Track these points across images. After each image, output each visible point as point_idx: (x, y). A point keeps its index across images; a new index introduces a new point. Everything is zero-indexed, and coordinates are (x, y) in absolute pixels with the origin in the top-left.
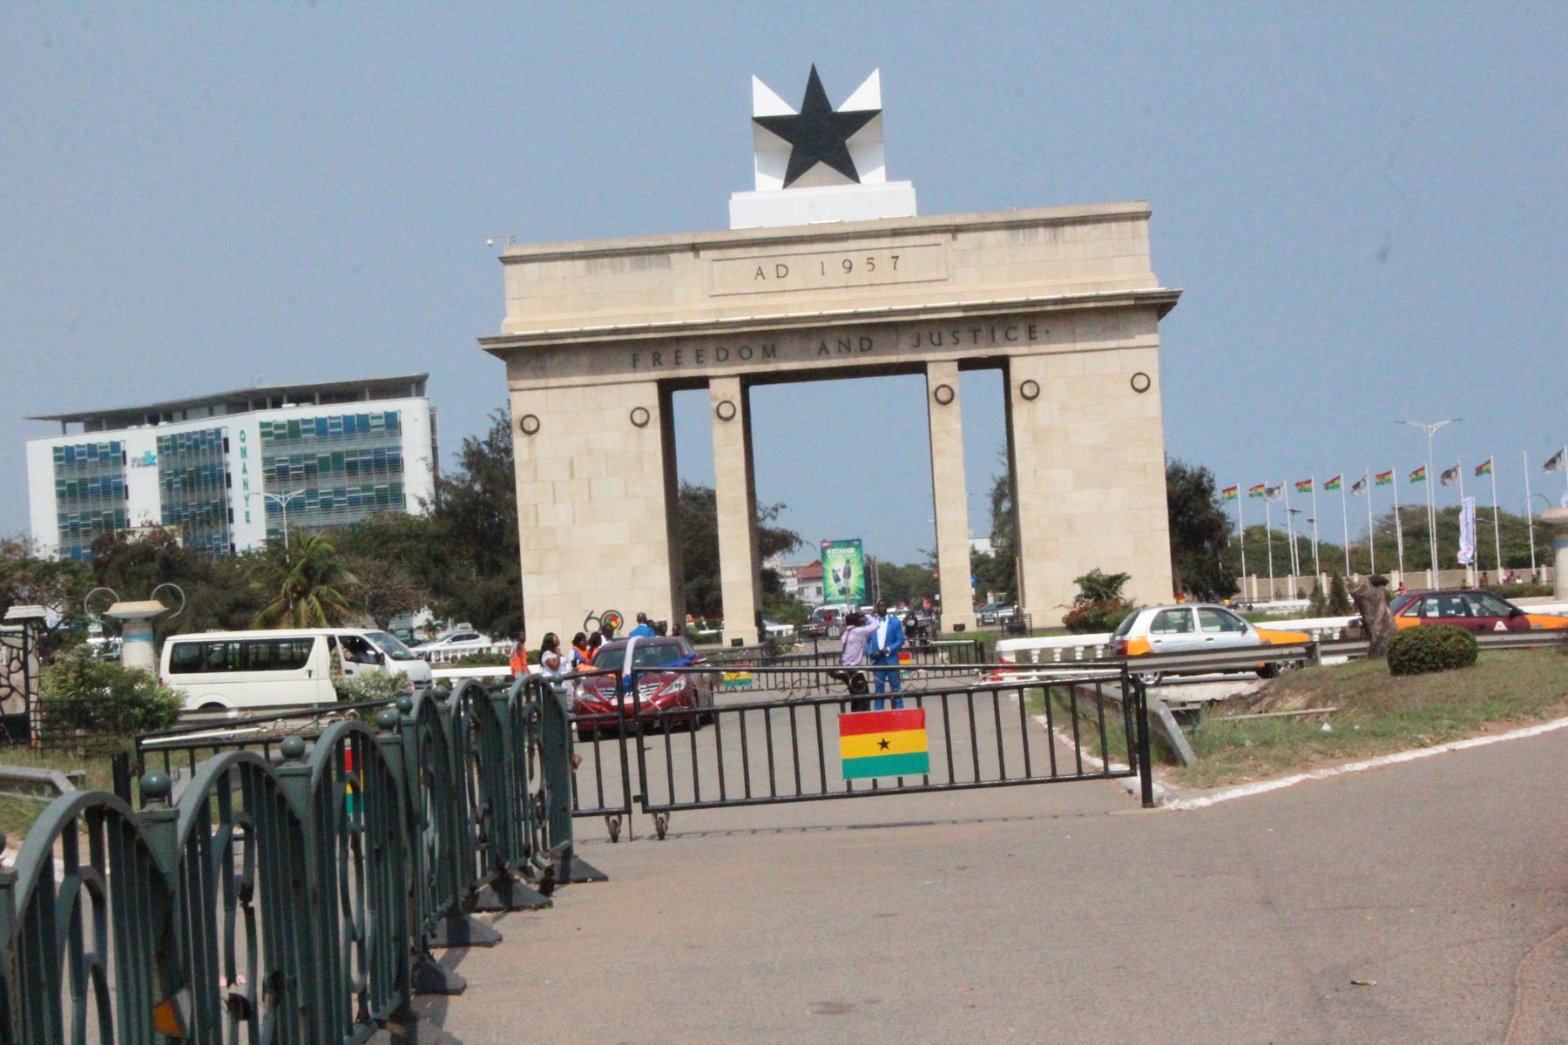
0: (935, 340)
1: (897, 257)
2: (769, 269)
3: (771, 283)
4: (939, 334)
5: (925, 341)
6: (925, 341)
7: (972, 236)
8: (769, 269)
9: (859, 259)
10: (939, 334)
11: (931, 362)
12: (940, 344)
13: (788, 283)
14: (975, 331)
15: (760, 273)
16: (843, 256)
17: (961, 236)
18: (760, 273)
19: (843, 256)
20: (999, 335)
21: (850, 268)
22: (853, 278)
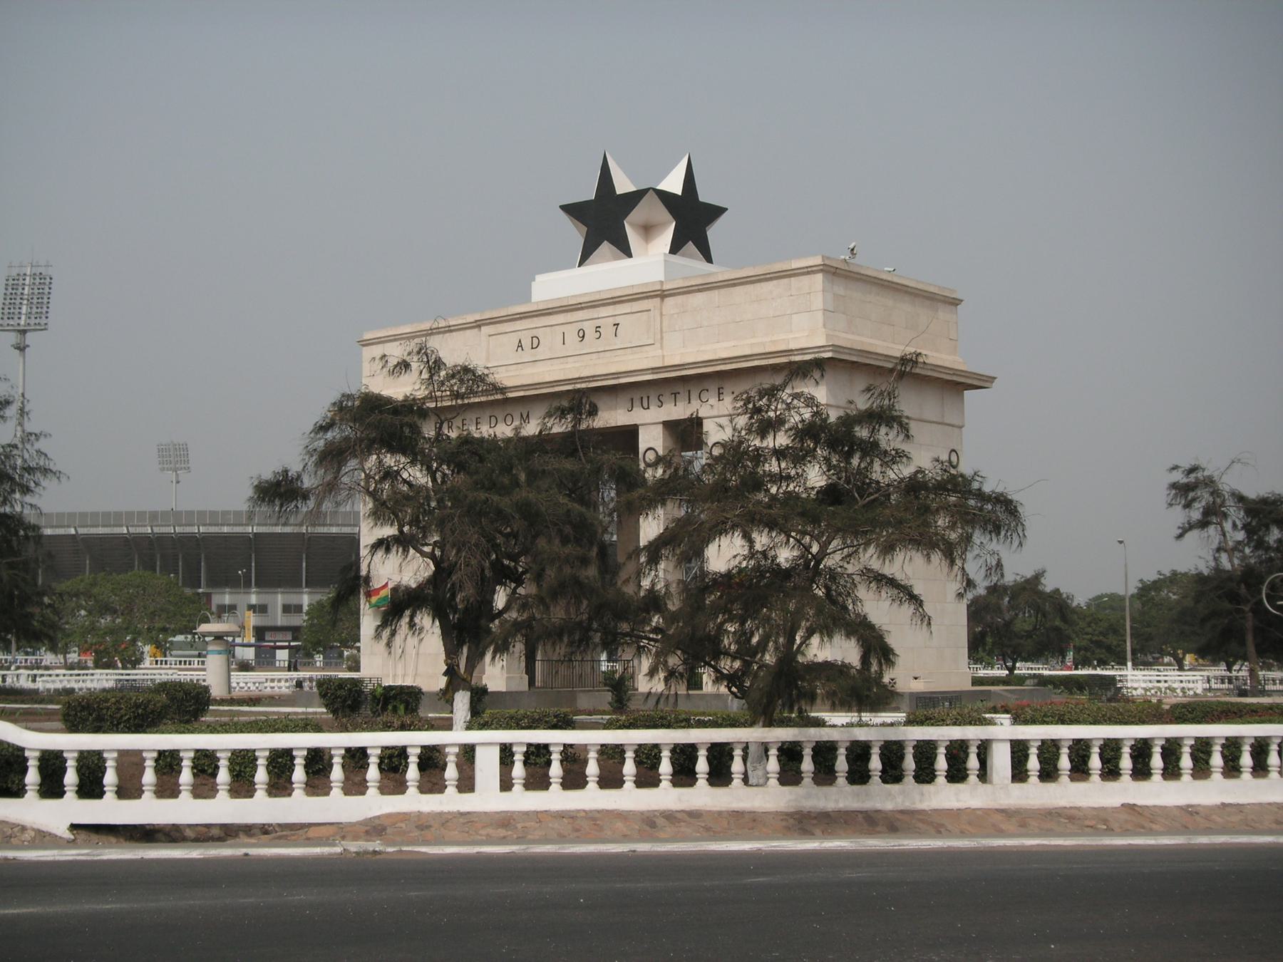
0: (645, 405)
1: (618, 324)
2: (526, 343)
3: (527, 355)
4: (648, 397)
5: (637, 403)
6: (637, 403)
7: (679, 299)
8: (526, 343)
9: (589, 328)
10: (648, 397)
11: (642, 425)
12: (648, 408)
13: (542, 353)
14: (675, 394)
15: (520, 345)
16: (580, 326)
17: (669, 301)
18: (520, 345)
19: (580, 326)
20: (694, 395)
21: (583, 336)
22: (585, 348)
